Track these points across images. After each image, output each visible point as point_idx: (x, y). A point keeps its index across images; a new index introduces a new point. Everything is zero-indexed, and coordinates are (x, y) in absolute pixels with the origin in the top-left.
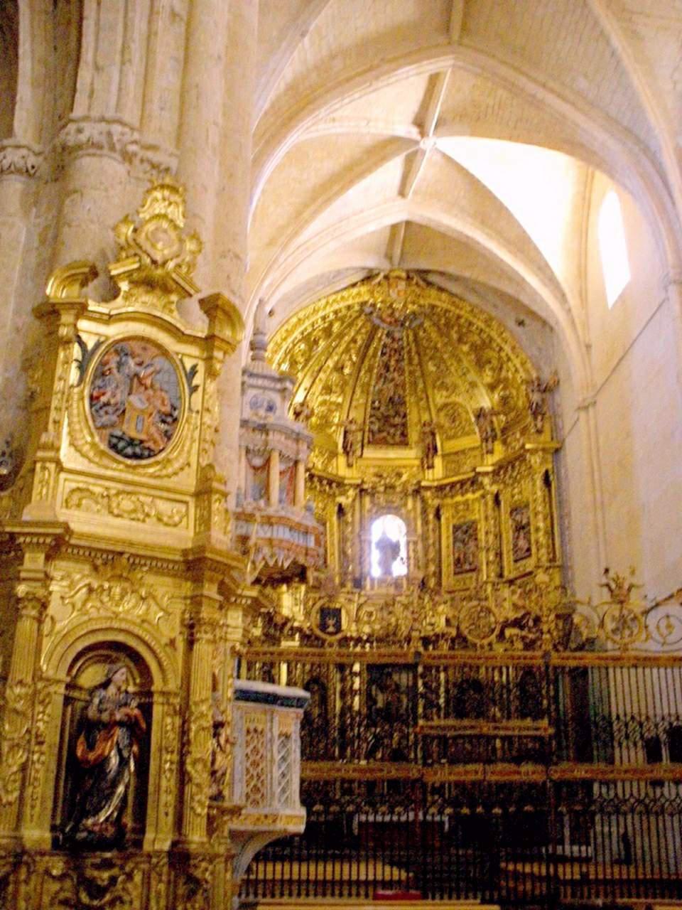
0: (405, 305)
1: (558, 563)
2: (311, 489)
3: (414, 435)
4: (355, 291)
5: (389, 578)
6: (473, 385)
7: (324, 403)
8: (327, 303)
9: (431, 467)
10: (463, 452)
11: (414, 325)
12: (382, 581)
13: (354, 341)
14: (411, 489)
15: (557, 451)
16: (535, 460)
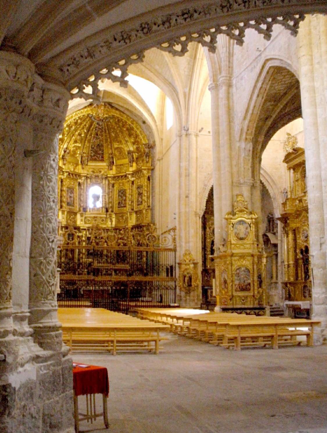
0: (104, 115)
1: (150, 208)
2: (69, 177)
3: (106, 156)
4: (86, 110)
5: (96, 208)
6: (127, 141)
7: (74, 147)
8: (76, 114)
9: (111, 169)
10: (122, 165)
11: (106, 121)
12: (93, 209)
13: (85, 125)
14: (104, 177)
15: (153, 170)
16: (145, 172)
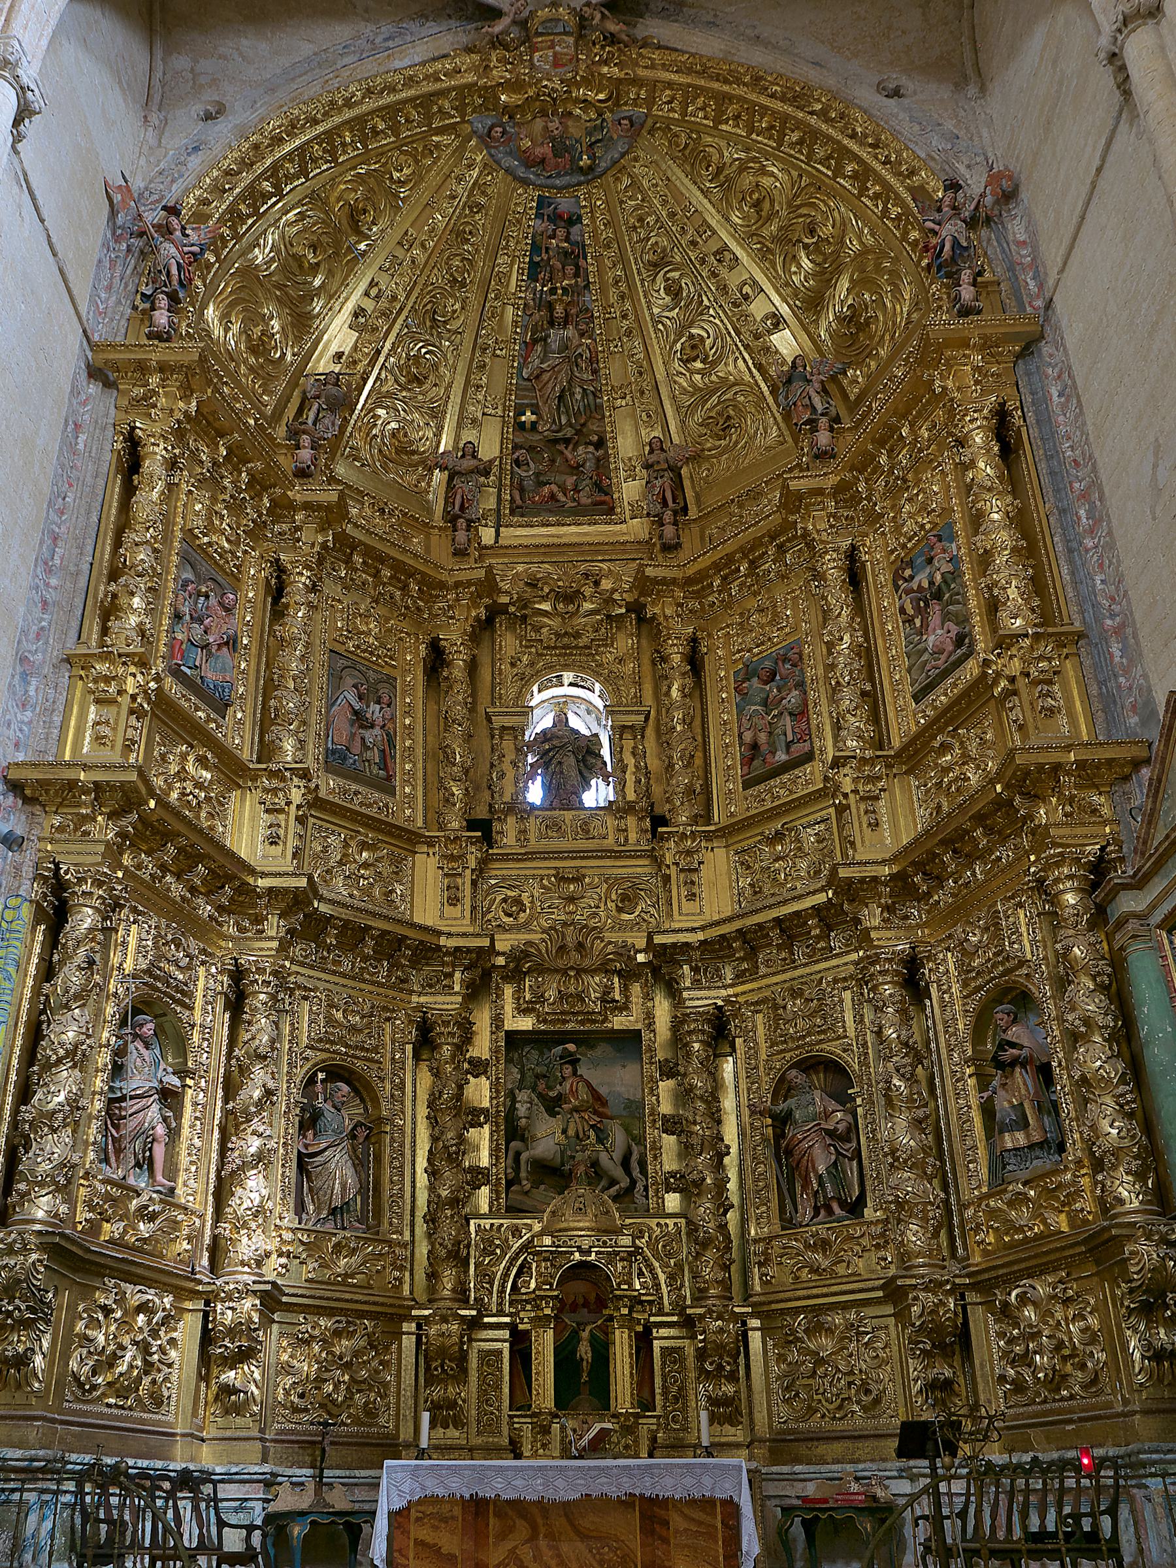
3: (630, 490)
